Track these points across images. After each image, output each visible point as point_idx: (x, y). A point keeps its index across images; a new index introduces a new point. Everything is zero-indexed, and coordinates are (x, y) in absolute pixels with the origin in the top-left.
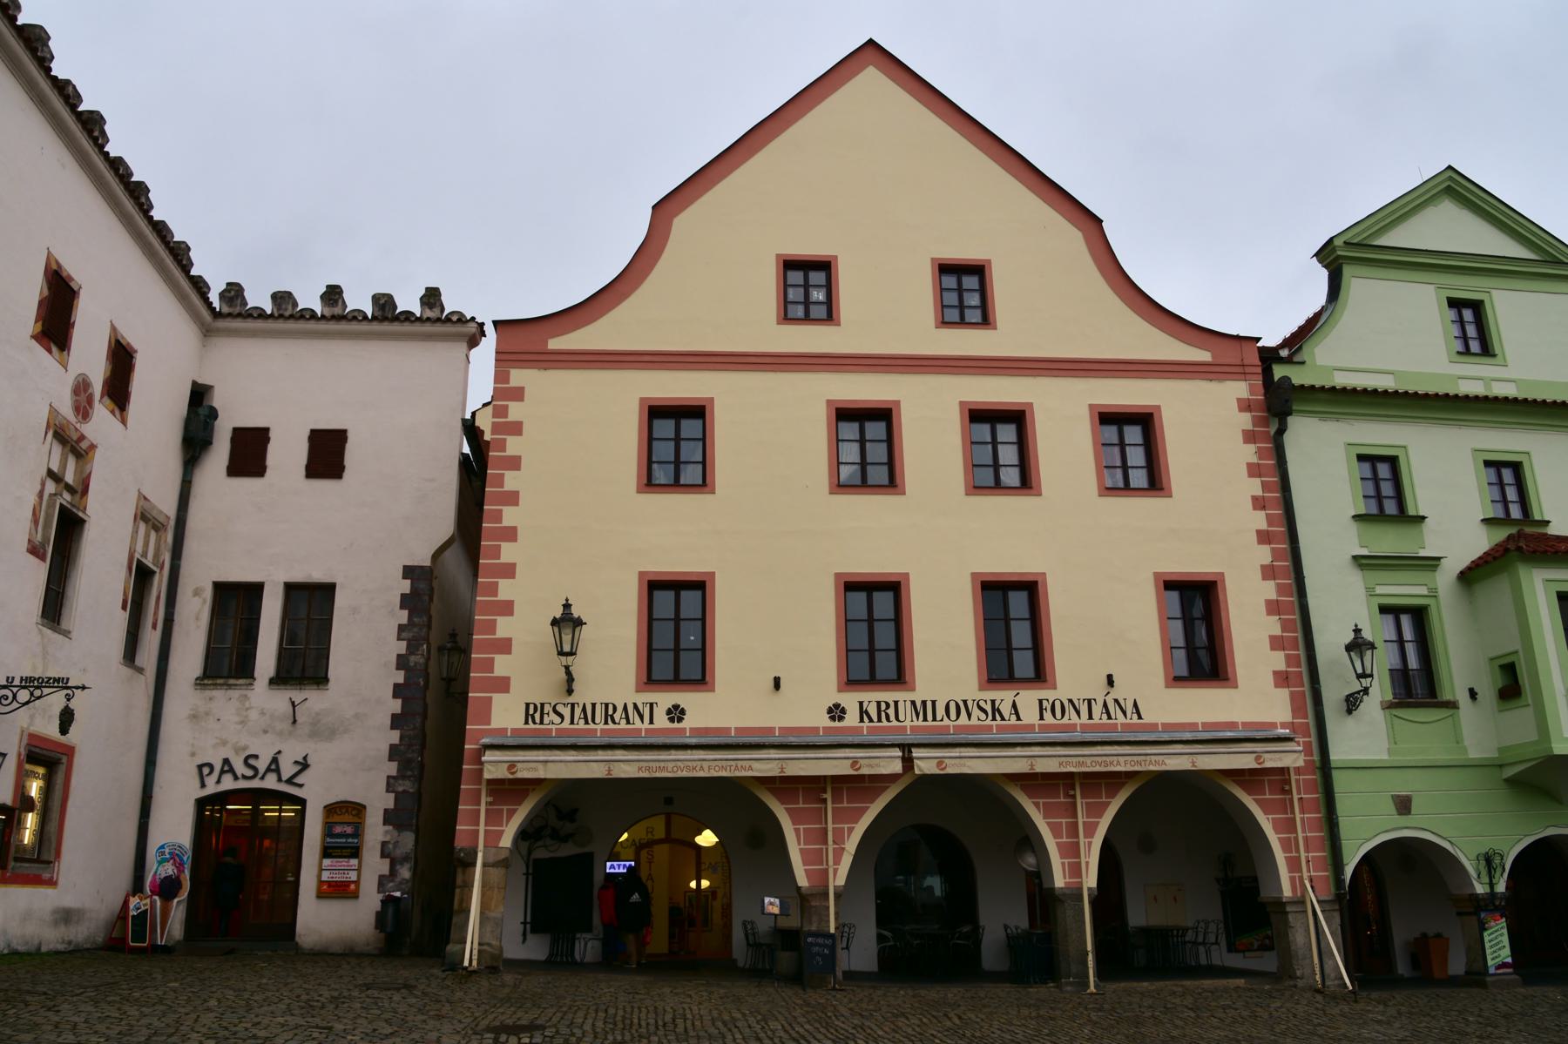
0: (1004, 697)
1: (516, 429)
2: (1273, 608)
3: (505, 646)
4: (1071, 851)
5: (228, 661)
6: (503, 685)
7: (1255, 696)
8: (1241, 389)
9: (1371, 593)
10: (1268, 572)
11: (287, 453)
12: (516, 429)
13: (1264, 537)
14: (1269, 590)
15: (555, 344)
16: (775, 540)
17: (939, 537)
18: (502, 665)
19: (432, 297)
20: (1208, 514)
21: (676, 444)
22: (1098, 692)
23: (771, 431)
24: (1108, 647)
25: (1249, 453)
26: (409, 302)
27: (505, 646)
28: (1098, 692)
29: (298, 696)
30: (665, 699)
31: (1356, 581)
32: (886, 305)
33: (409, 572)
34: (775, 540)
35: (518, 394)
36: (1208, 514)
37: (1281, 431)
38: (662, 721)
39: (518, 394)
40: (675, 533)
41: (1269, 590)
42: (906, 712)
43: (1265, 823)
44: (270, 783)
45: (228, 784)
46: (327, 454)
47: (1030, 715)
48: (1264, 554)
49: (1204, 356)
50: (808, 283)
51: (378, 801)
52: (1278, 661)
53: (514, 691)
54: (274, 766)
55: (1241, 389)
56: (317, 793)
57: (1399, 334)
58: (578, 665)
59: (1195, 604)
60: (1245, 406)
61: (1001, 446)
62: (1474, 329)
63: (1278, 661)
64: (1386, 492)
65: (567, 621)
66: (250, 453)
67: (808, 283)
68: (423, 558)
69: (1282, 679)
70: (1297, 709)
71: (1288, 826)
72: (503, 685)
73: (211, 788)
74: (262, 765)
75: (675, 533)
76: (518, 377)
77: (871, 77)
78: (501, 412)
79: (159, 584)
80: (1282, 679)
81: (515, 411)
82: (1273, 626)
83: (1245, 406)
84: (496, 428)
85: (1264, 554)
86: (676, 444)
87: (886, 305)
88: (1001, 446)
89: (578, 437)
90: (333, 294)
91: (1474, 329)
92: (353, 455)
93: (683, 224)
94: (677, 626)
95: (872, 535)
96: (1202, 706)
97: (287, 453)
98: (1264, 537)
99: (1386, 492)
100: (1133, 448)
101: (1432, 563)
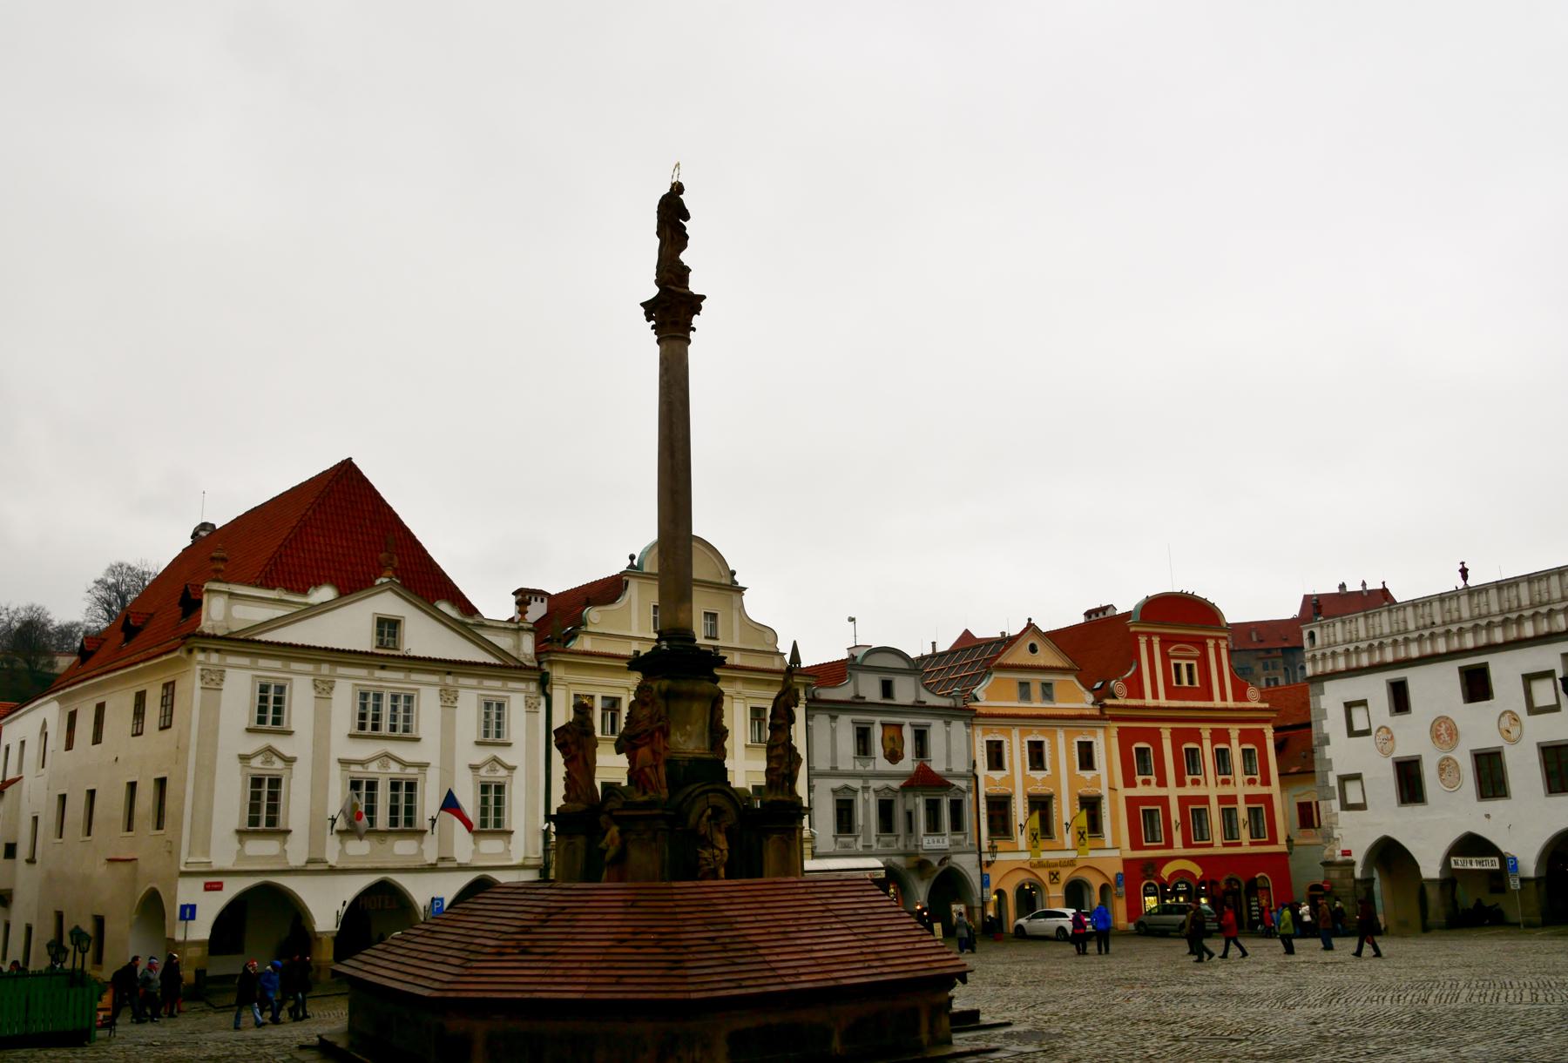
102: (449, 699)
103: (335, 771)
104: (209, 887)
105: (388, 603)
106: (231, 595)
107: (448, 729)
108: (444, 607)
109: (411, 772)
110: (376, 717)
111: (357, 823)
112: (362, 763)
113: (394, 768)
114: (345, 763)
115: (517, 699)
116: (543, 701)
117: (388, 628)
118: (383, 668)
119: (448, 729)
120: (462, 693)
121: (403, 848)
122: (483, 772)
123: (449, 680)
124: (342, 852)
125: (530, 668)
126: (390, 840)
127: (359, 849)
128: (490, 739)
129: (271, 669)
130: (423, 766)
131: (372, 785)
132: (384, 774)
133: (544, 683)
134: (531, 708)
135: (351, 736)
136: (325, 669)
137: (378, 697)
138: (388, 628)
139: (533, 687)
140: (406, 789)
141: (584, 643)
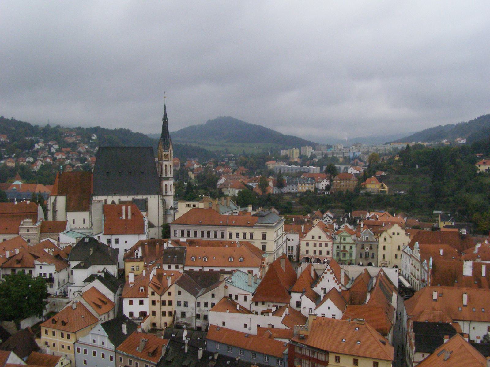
7: (330, 255)
11: (291, 240)
16: (311, 249)
17: (318, 249)
21: (307, 244)
23: (311, 244)
24: (324, 253)
32: (316, 238)
34: (311, 249)
36: (329, 248)
40: (307, 248)
46: (293, 240)
50: (313, 237)
53: (301, 254)
56: (293, 255)
59: (328, 253)
61: (321, 245)
62: (344, 239)
64: (338, 247)
66: (289, 240)
67: (313, 237)
75: (307, 248)
86: (307, 244)
87: (316, 238)
88: (321, 245)
94: (307, 252)
95: (315, 248)
96: (328, 256)
97: (291, 240)
100: (326, 245)
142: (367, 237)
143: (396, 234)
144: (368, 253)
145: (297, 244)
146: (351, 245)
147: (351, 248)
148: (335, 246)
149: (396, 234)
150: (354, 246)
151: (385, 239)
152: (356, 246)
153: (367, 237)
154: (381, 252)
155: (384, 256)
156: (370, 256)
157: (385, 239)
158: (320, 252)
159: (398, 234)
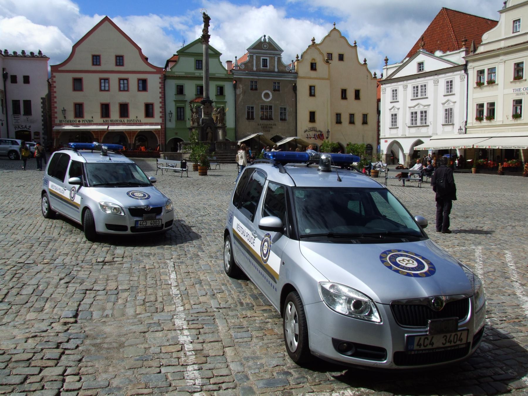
0: (122, 119)
1: (55, 82)
2: (161, 107)
3: (56, 113)
4: (130, 139)
5: (16, 111)
6: (56, 118)
8: (159, 76)
9: (176, 105)
10: (161, 103)
11: (20, 79)
12: (55, 82)
13: (160, 98)
14: (161, 105)
15: (60, 69)
17: (115, 98)
18: (56, 115)
19: (40, 52)
20: (153, 95)
22: (135, 119)
25: (160, 85)
26: (36, 53)
27: (56, 113)
28: (135, 119)
29: (28, 117)
30: (78, 119)
31: (174, 103)
32: (108, 63)
33: (42, 98)
35: (55, 77)
37: (164, 83)
38: (77, 122)
39: (55, 77)
40: (78, 97)
41: (161, 105)
42: (109, 121)
43: (157, 136)
44: (25, 129)
45: (19, 129)
46: (26, 79)
47: (126, 122)
48: (160, 100)
49: (155, 70)
50: (96, 59)
51: (41, 132)
52: (161, 115)
54: (26, 127)
55: (159, 76)
56: (32, 130)
57: (187, 66)
58: (66, 115)
60: (160, 78)
63: (161, 115)
65: (64, 111)
67: (96, 59)
68: (44, 96)
69: (161, 117)
70: (163, 121)
71: (159, 136)
72: (56, 118)
73: (17, 130)
74: (24, 127)
75: (78, 97)
76: (55, 74)
77: (107, 22)
78: (52, 79)
79: (4, 101)
80: (161, 117)
81: (54, 79)
82: (161, 110)
83: (160, 78)
84: (52, 82)
85: (160, 100)
86: (78, 85)
87: (108, 63)
89: (64, 82)
90: (23, 52)
91: (199, 65)
92: (31, 79)
93: (77, 49)
94: (79, 110)
95: (105, 98)
97: (20, 79)
98: (160, 98)
99: (180, 90)
100: (143, 85)
101: (186, 101)
102: (436, 83)
103: (408, 109)
104: (386, 142)
105: (421, 57)
106: (387, 69)
107: (436, 92)
108: (438, 53)
109: (425, 109)
110: (417, 93)
111: (413, 124)
112: (414, 107)
113: (421, 107)
114: (410, 108)
115: (457, 77)
116: (466, 76)
117: (421, 65)
118: (419, 78)
119: (436, 92)
120: (440, 80)
121: (424, 130)
122: (446, 105)
123: (436, 77)
124: (409, 132)
125: (460, 66)
126: (420, 128)
127: (413, 130)
128: (419, 97)
129: (394, 86)
130: (429, 105)
131: (416, 113)
132: (418, 109)
133: (466, 70)
134: (462, 79)
135: (412, 100)
136: (405, 82)
137: (417, 87)
138: (421, 65)
139: (463, 72)
140: (424, 113)
141: (481, 49)
142: (265, 61)
143: (335, 57)
144: (271, 107)
145: (44, 92)
146: (221, 83)
147: (221, 91)
148: (172, 85)
149: (335, 57)
150: (228, 88)
151: (313, 67)
152: (235, 87)
153: (265, 61)
154: (305, 104)
155: (312, 117)
156: (276, 114)
157: (313, 67)
158: (124, 110)
159: (341, 57)
